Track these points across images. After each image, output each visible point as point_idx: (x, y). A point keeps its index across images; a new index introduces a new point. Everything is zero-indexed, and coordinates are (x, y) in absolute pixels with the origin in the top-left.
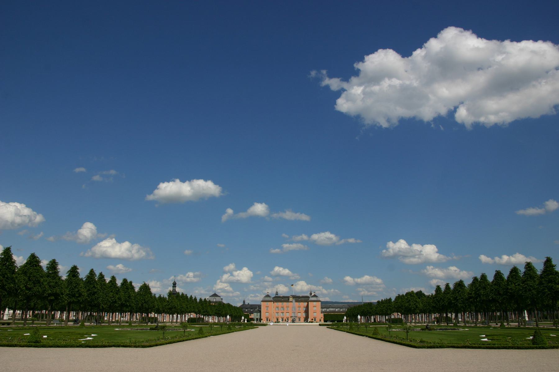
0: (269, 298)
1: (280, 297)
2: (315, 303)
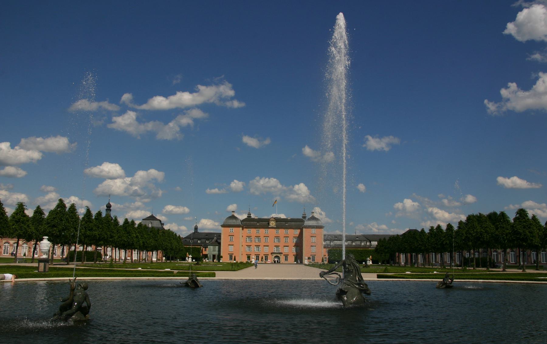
0: (234, 221)
1: (254, 220)
2: (314, 231)
